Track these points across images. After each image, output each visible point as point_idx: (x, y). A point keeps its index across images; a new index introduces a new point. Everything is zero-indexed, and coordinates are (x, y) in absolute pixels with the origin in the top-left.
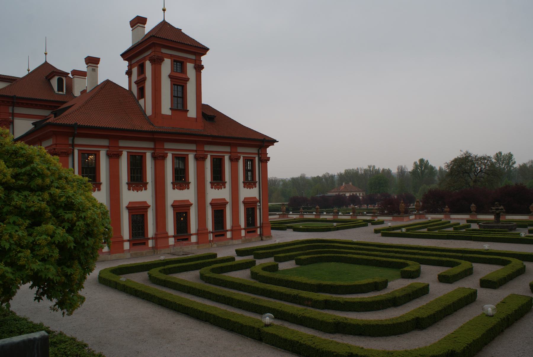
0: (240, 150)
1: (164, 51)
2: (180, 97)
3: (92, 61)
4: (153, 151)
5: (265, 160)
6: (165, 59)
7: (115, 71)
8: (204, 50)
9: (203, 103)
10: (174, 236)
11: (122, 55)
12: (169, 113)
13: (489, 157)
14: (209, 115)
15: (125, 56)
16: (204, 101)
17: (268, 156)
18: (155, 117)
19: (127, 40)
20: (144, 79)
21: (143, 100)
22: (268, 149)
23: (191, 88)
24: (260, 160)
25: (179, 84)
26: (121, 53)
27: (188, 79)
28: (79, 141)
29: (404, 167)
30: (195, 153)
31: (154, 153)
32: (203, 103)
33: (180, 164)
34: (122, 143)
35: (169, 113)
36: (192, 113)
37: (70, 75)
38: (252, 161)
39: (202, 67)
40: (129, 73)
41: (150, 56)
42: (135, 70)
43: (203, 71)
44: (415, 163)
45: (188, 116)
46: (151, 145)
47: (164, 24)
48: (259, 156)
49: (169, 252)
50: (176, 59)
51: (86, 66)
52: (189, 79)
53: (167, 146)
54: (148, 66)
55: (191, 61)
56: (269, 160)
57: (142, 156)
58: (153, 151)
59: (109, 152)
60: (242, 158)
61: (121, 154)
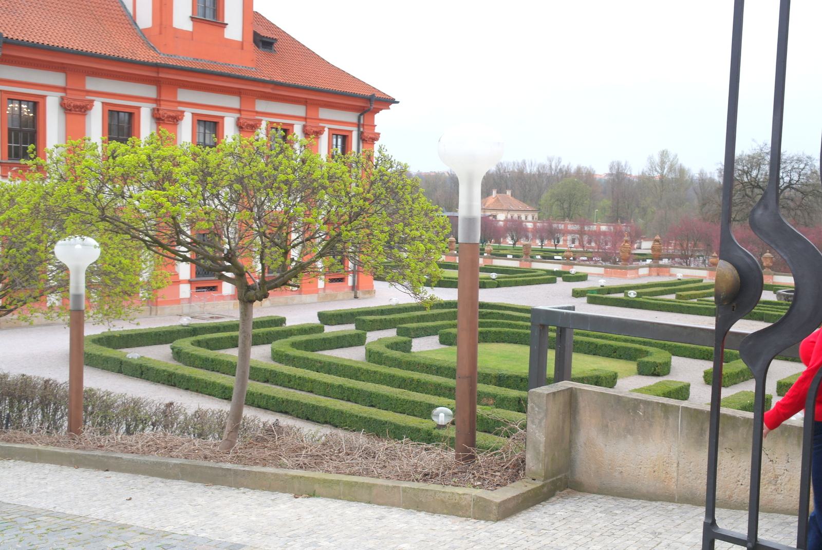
0: (324, 113)
4: (154, 106)
5: (368, 138)
9: (255, 9)
10: (190, 282)
12: (188, 26)
13: (809, 158)
14: (265, 40)
16: (256, 8)
17: (377, 130)
18: (160, 33)
22: (377, 116)
24: (362, 138)
29: (623, 164)
30: (238, 115)
31: (158, 110)
33: (207, 136)
34: (92, 84)
36: (234, 30)
38: (345, 138)
44: (650, 159)
46: (150, 91)
48: (359, 130)
49: (180, 313)
53: (184, 95)
56: (377, 139)
57: (131, 115)
58: (154, 106)
59: (66, 101)
60: (326, 130)
61: (92, 106)
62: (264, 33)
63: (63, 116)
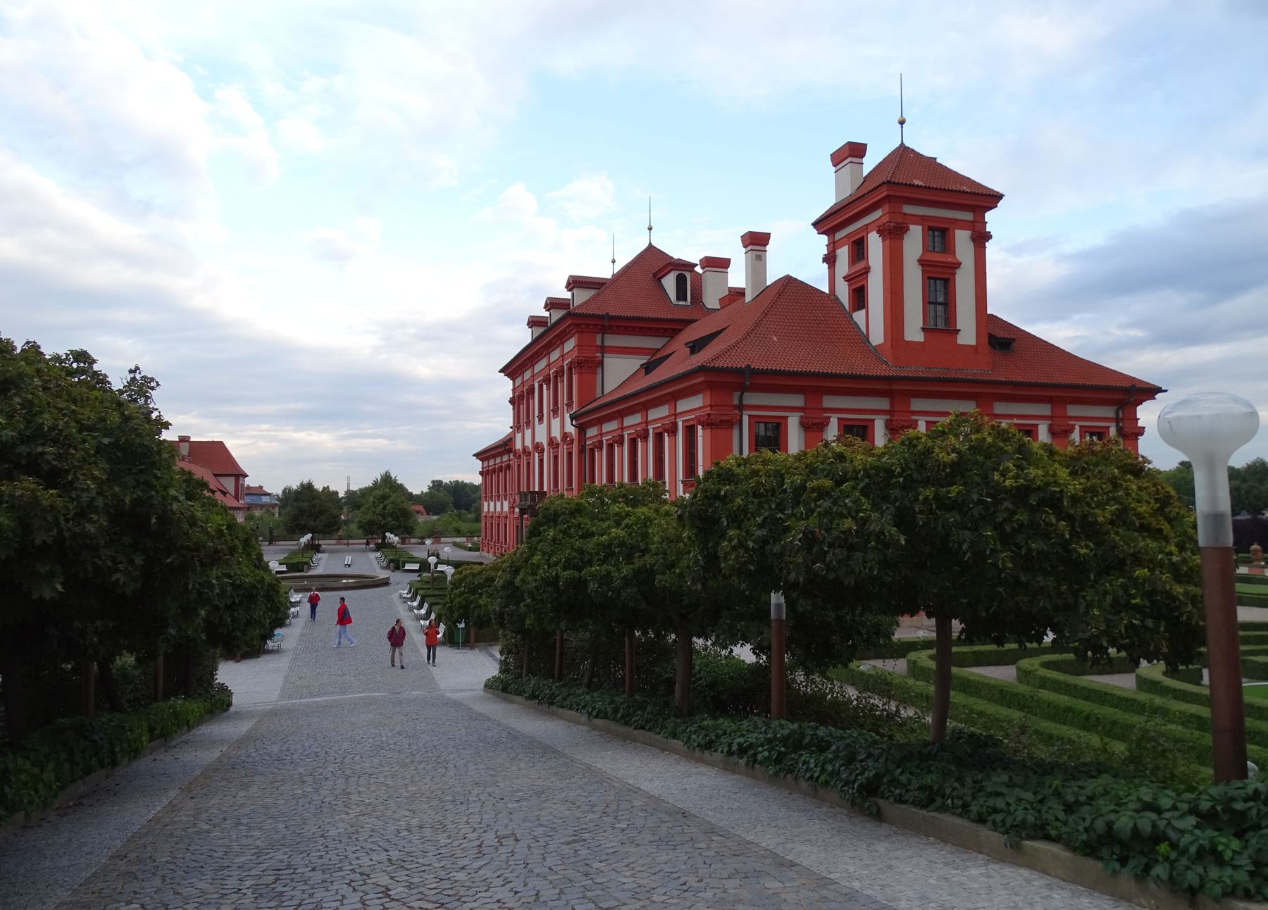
1: (908, 209)
2: (941, 304)
3: (756, 241)
6: (911, 227)
7: (802, 257)
8: (993, 198)
9: (989, 312)
11: (815, 224)
12: (919, 337)
14: (1002, 339)
15: (821, 225)
16: (990, 310)
19: (825, 192)
20: (867, 270)
21: (863, 312)
23: (964, 283)
25: (940, 276)
26: (813, 220)
27: (958, 265)
28: (752, 399)
32: (989, 312)
34: (829, 402)
35: (919, 337)
36: (967, 334)
37: (698, 269)
39: (988, 236)
40: (830, 259)
41: (880, 223)
42: (843, 253)
43: (989, 245)
45: (959, 342)
47: (903, 154)
50: (933, 224)
51: (744, 250)
52: (960, 264)
54: (875, 244)
55: (962, 225)
62: (1001, 334)
63: (803, 434)
